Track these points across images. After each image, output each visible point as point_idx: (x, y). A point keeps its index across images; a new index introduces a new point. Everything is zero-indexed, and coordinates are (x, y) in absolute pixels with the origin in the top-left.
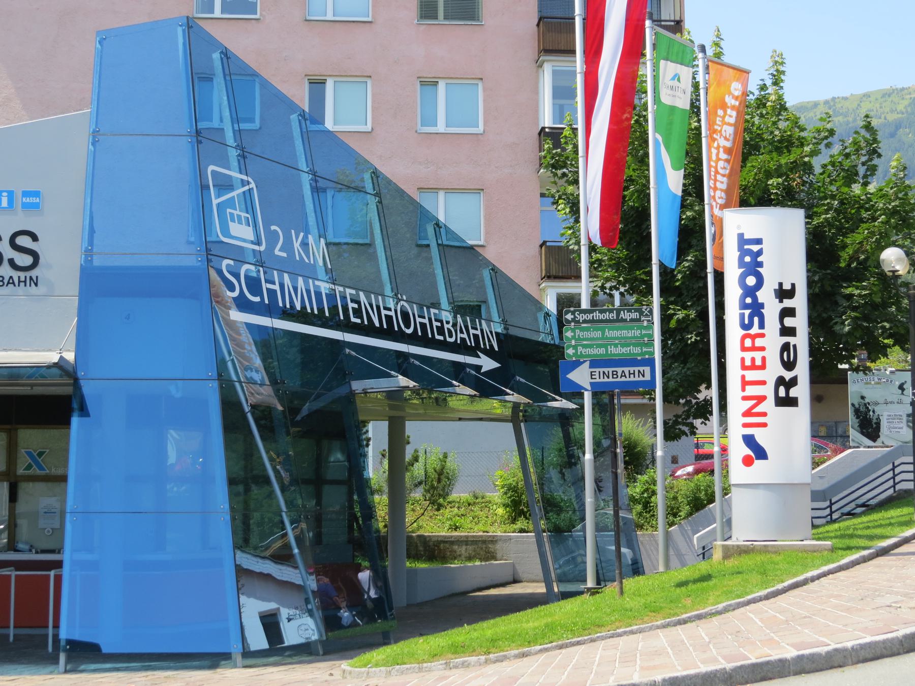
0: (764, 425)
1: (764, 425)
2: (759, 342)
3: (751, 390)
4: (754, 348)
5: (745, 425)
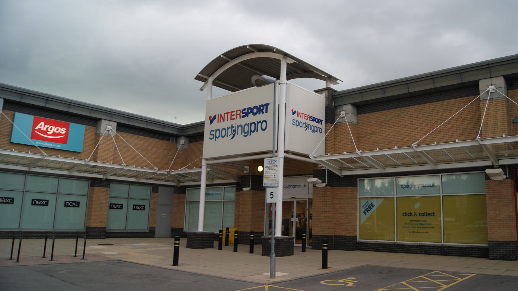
0: (218, 122)
1: (218, 122)
2: (238, 116)
3: (226, 115)
4: (237, 115)
5: (218, 115)
